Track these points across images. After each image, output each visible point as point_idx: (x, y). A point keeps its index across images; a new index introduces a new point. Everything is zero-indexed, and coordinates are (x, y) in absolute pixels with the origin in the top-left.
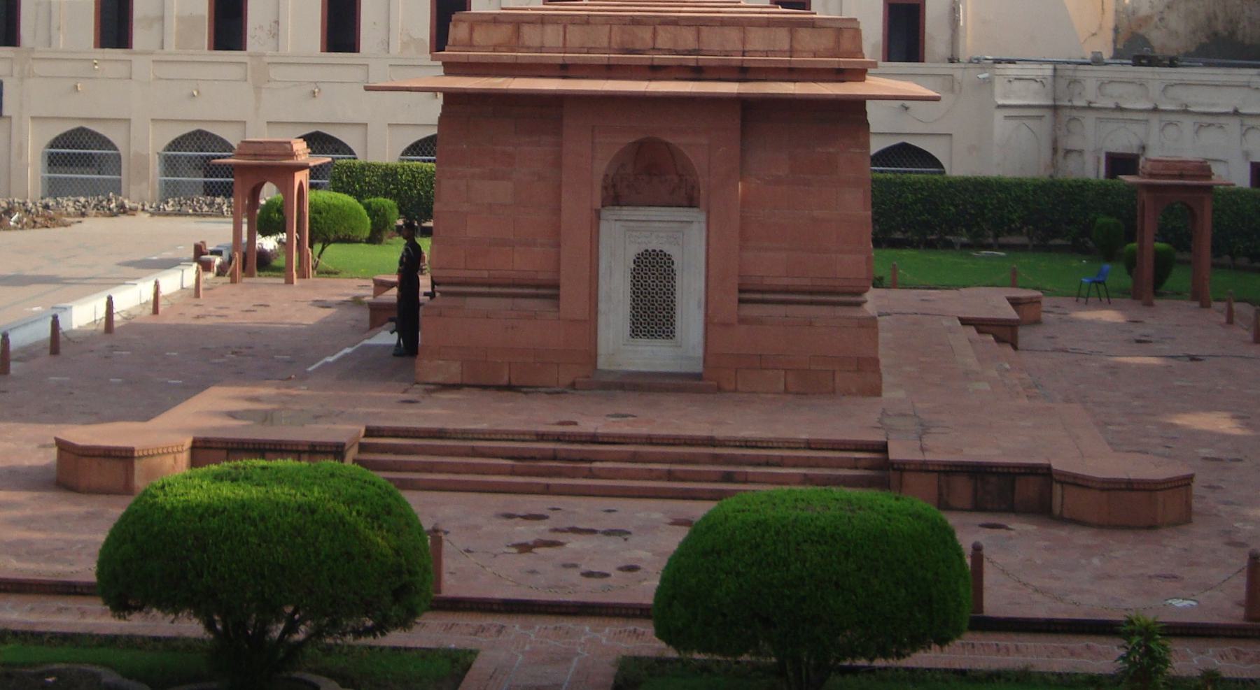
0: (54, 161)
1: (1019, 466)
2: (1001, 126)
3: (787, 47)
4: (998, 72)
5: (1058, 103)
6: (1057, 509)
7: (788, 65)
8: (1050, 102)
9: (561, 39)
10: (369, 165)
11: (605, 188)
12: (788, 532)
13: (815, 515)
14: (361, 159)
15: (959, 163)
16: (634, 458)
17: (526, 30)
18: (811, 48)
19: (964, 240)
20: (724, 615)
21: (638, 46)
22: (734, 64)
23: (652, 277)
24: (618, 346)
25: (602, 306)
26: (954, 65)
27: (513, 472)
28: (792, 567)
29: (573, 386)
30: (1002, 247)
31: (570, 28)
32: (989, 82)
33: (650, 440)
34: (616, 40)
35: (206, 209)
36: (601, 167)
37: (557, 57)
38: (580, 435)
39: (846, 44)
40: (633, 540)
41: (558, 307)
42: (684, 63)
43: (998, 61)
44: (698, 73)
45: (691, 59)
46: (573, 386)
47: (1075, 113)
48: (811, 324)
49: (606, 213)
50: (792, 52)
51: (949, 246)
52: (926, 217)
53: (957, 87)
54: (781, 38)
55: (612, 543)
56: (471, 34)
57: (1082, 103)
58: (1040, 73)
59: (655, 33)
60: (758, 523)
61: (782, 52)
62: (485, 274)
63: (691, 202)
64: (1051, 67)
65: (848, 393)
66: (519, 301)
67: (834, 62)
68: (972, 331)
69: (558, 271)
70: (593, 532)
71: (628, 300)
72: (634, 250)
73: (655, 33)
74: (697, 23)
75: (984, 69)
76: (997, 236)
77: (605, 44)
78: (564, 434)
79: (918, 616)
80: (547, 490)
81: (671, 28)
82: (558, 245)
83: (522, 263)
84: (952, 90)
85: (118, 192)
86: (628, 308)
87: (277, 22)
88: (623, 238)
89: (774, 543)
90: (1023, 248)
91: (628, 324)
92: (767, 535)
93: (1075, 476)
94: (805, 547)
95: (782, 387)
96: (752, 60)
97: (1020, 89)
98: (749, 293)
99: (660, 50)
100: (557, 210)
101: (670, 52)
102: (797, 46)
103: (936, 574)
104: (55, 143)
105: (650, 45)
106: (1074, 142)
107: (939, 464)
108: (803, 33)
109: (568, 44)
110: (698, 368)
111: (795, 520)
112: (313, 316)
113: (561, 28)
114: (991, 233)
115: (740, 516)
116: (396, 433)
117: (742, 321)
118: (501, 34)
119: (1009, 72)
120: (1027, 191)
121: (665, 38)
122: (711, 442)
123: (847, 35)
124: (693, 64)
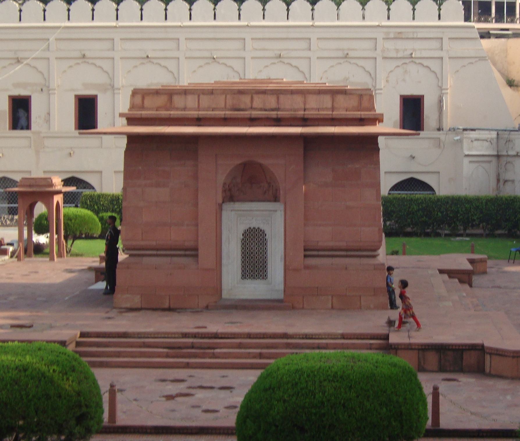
1: (466, 345)
2: (467, 167)
3: (329, 105)
4: (465, 136)
5: (499, 154)
6: (487, 370)
7: (331, 117)
8: (495, 153)
9: (197, 103)
10: (103, 195)
11: (224, 191)
12: (315, 376)
13: (331, 365)
14: (98, 191)
15: (443, 189)
16: (240, 346)
18: (344, 107)
19: (447, 232)
20: (277, 426)
21: (242, 106)
22: (299, 116)
24: (234, 283)
25: (224, 261)
26: (441, 132)
27: (167, 356)
28: (317, 396)
29: (207, 308)
30: (468, 235)
31: (202, 96)
32: (460, 141)
33: (249, 336)
34: (230, 102)
36: (221, 178)
37: (194, 114)
38: (208, 334)
39: (365, 103)
40: (235, 392)
41: (197, 261)
42: (269, 116)
43: (465, 130)
44: (278, 122)
45: (273, 114)
46: (207, 308)
47: (509, 159)
48: (346, 268)
49: (225, 206)
50: (333, 109)
51: (438, 235)
52: (424, 218)
53: (442, 144)
54: (327, 101)
55: (223, 394)
57: (514, 153)
58: (489, 136)
59: (252, 98)
60: (297, 371)
61: (327, 109)
62: (154, 243)
63: (276, 199)
64: (496, 133)
65: (369, 308)
66: (175, 259)
67: (358, 114)
68: (446, 276)
69: (197, 240)
70: (212, 388)
71: (240, 257)
72: (242, 228)
73: (252, 98)
74: (278, 93)
75: (457, 134)
76: (465, 229)
77: (223, 105)
78: (198, 333)
79: (394, 424)
80: (187, 366)
81: (261, 96)
82: (197, 225)
83: (177, 236)
84: (439, 146)
86: (240, 262)
88: (236, 220)
89: (306, 382)
90: (481, 236)
91: (240, 271)
92: (302, 378)
93: (497, 350)
94: (325, 383)
95: (330, 306)
96: (309, 114)
97: (478, 146)
98: (310, 251)
99: (255, 109)
100: (196, 205)
101: (261, 110)
102: (336, 105)
103: (405, 399)
105: (249, 105)
106: (509, 176)
107: (418, 345)
108: (340, 98)
109: (201, 105)
110: (280, 296)
111: (320, 368)
113: (196, 96)
114: (462, 228)
115: (287, 367)
116: (98, 335)
117: (307, 267)
118: (162, 100)
119: (471, 136)
120: (482, 203)
121: (258, 102)
122: (285, 336)
123: (365, 99)
124: (275, 116)
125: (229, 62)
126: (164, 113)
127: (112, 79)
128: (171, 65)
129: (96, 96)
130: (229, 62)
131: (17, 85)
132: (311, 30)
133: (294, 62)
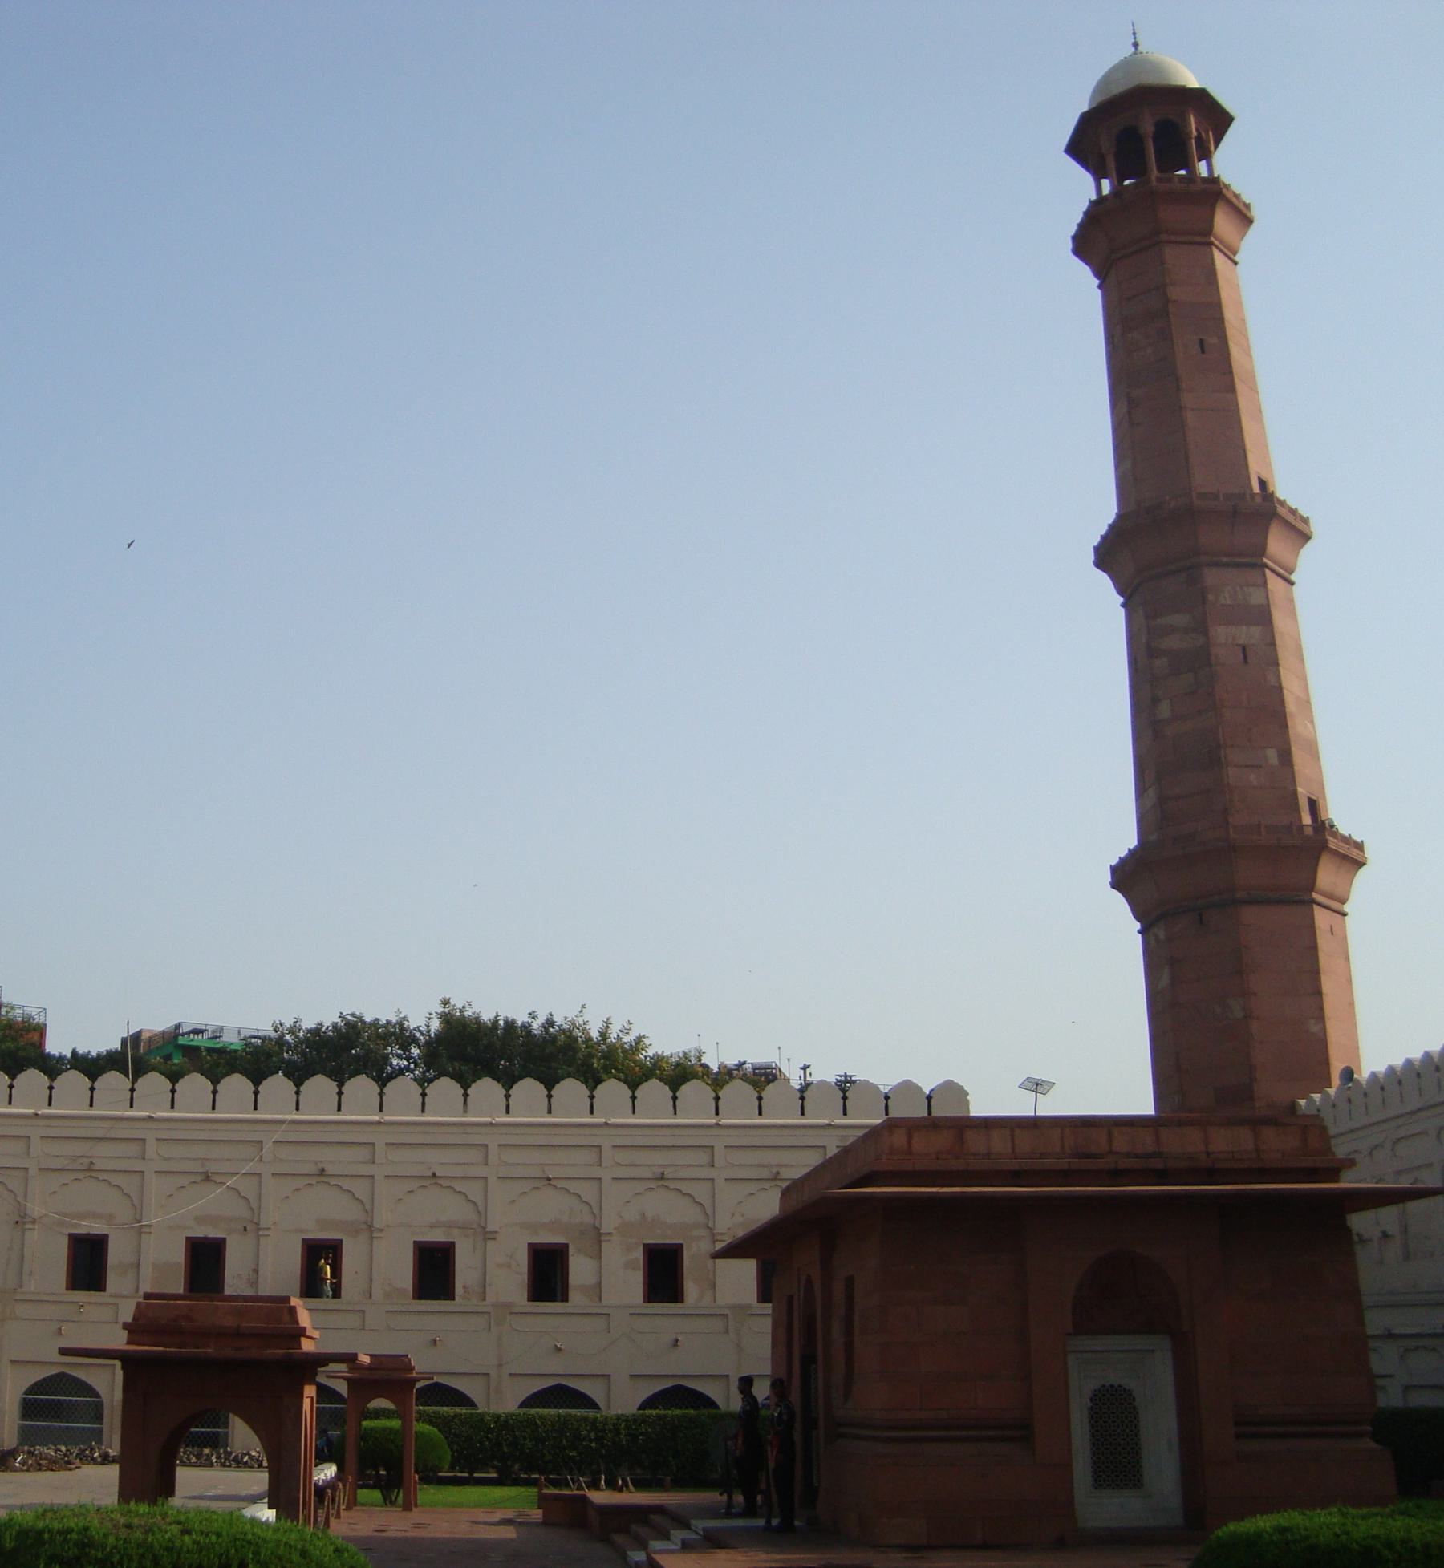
0: (30, 1409)
17: (969, 1135)
23: (1114, 1412)
31: (1018, 1132)
35: (194, 1460)
44: (1162, 1177)
56: (909, 1142)
73: (1110, 1134)
85: (100, 1442)
87: (256, 1271)
104: (34, 1389)
112: (509, 1533)
125: (573, 1186)
126: (955, 1164)
127: (369, 1213)
128: (474, 1190)
129: (341, 1241)
130: (573, 1186)
131: (201, 1220)
132: (715, 1131)
133: (685, 1187)
